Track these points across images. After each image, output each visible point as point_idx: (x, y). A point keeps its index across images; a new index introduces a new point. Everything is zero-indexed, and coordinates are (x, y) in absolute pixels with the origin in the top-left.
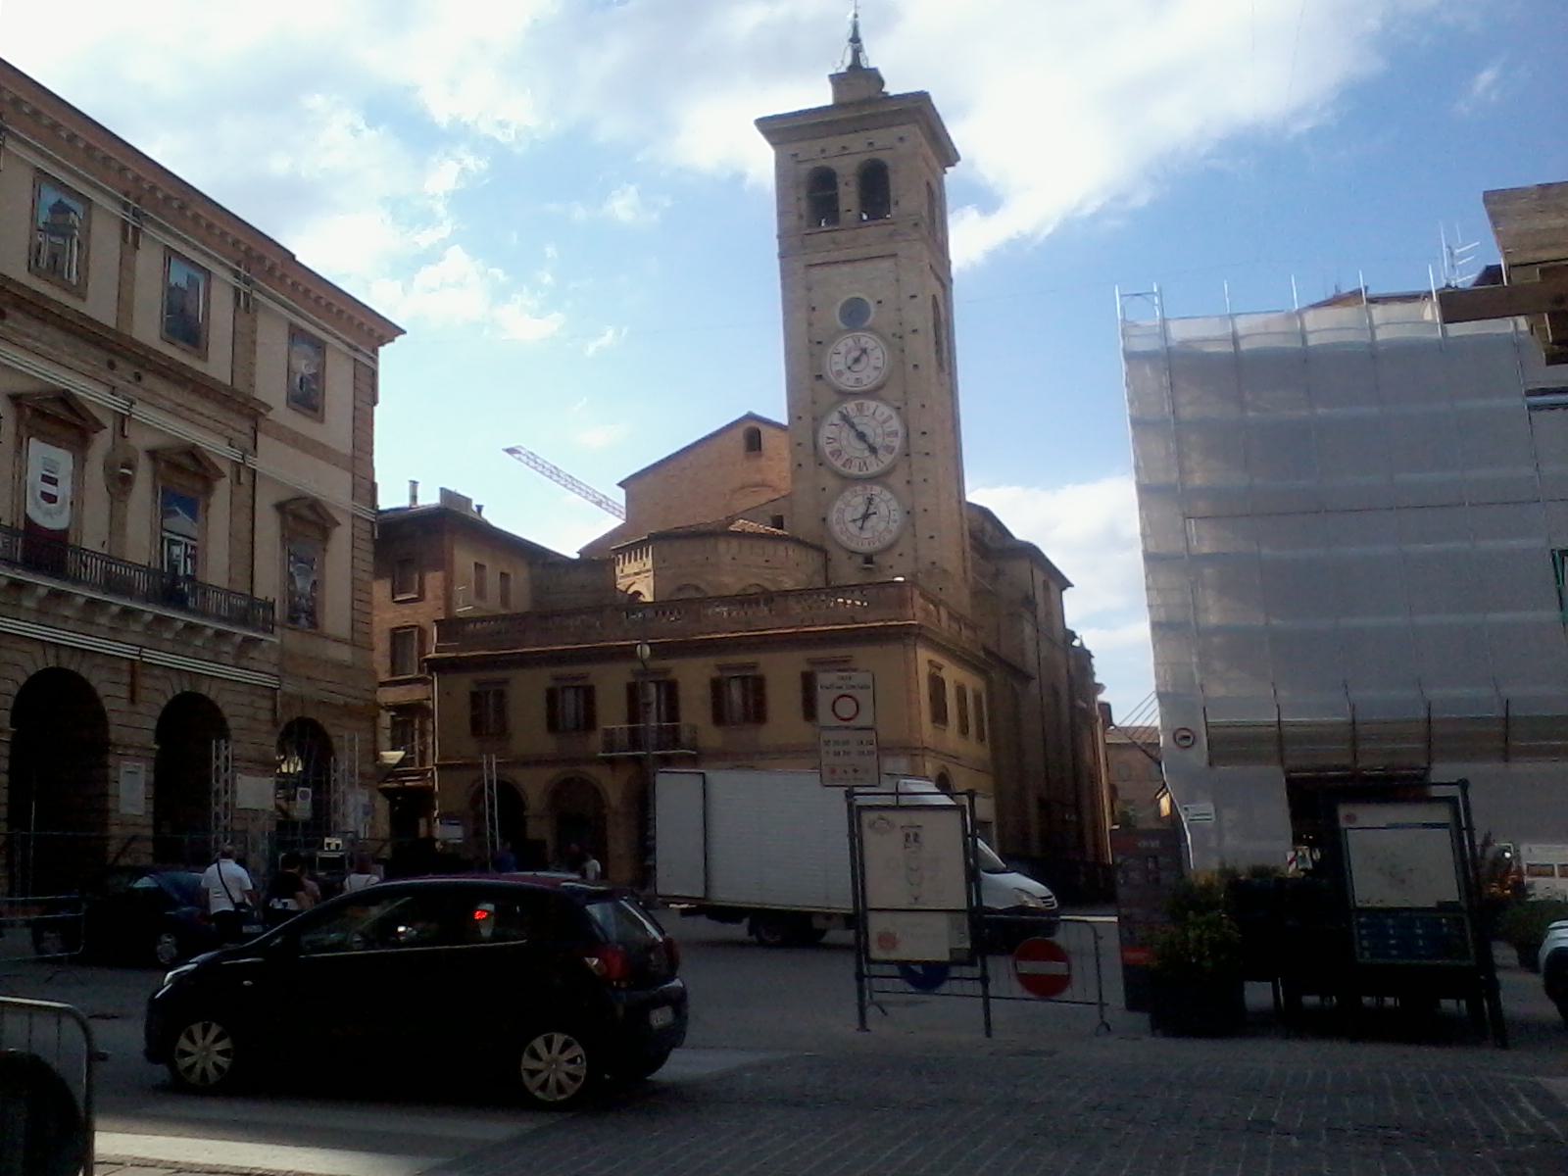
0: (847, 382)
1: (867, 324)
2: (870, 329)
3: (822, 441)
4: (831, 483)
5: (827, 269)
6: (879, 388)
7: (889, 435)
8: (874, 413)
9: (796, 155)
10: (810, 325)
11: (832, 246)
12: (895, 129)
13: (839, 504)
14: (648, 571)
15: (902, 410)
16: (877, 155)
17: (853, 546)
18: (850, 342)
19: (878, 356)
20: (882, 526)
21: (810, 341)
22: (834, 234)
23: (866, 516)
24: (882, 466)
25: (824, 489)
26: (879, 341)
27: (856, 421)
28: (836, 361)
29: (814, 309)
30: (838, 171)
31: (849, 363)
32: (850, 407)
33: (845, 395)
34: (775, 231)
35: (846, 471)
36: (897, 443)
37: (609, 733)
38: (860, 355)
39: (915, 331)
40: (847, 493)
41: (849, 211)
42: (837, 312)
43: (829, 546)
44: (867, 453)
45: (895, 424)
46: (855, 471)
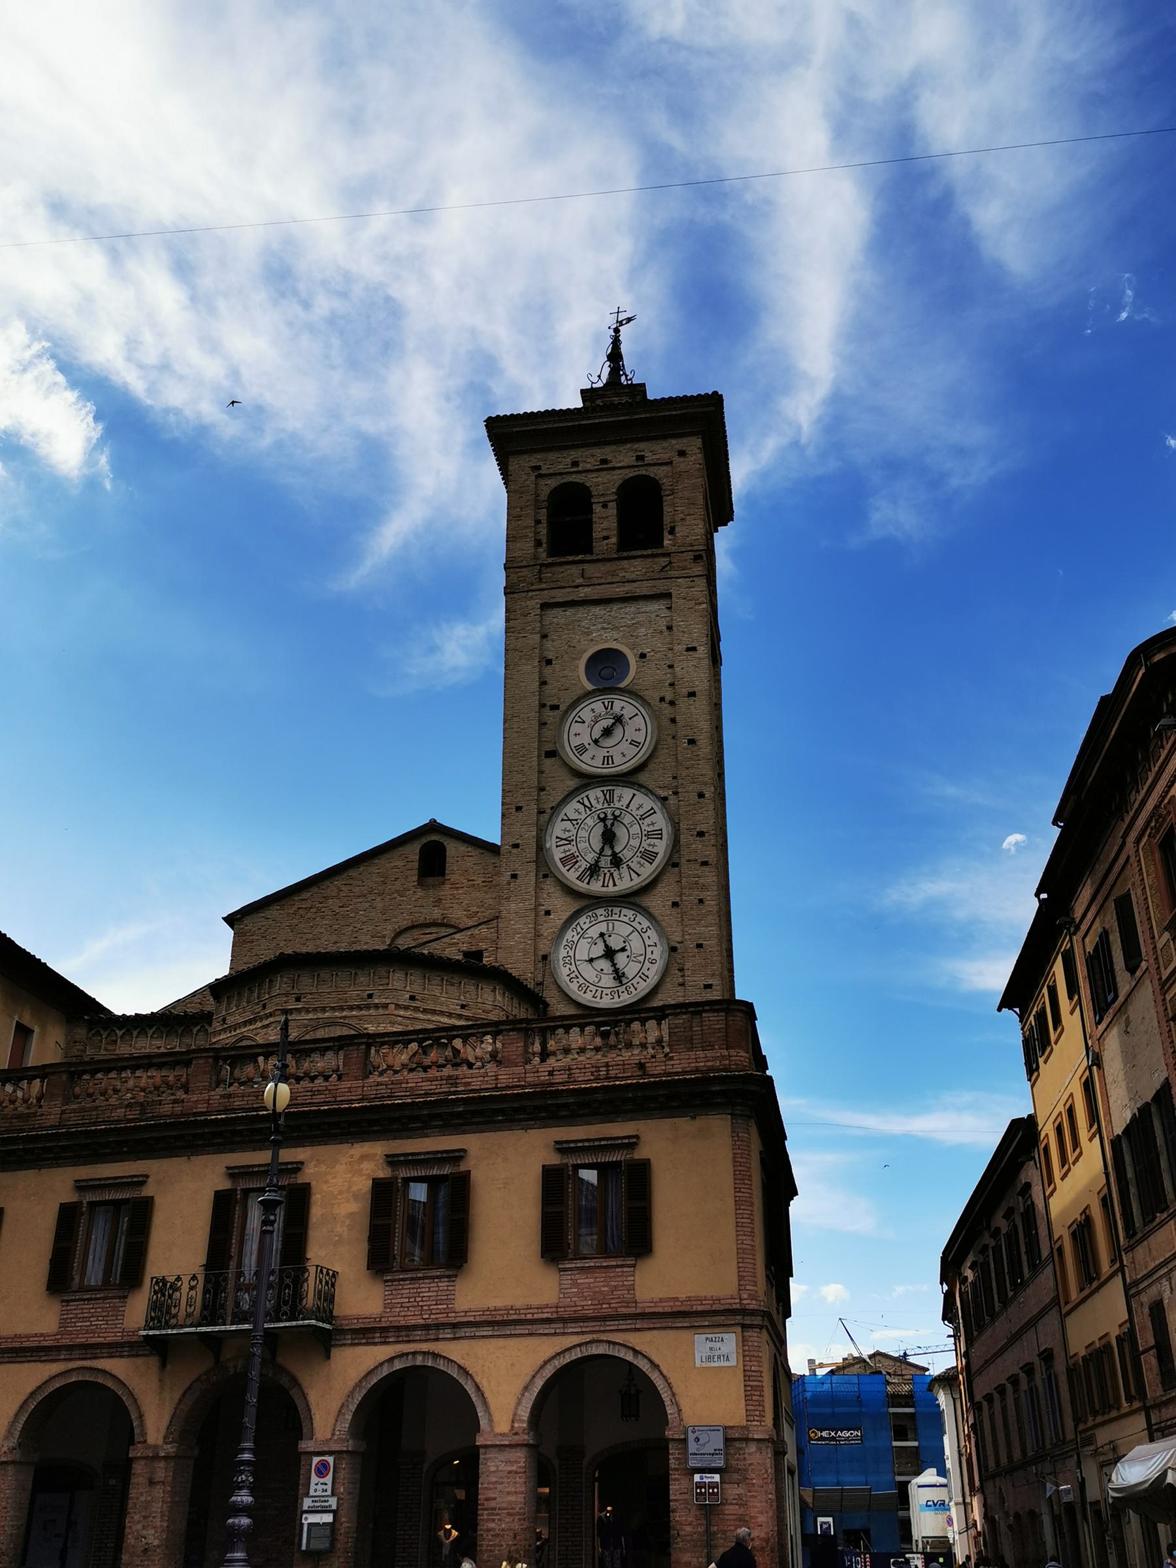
0: (591, 762)
3: (551, 843)
5: (570, 612)
6: (641, 767)
7: (648, 835)
10: (543, 683)
12: (674, 442)
13: (570, 935)
15: (672, 801)
16: (652, 472)
19: (639, 727)
22: (586, 566)
25: (548, 913)
28: (579, 732)
29: (549, 662)
31: (597, 733)
32: (595, 795)
33: (589, 780)
36: (661, 847)
37: (164, 1287)
38: (613, 724)
39: (692, 694)
40: (583, 920)
41: (606, 538)
43: (550, 996)
45: (660, 821)
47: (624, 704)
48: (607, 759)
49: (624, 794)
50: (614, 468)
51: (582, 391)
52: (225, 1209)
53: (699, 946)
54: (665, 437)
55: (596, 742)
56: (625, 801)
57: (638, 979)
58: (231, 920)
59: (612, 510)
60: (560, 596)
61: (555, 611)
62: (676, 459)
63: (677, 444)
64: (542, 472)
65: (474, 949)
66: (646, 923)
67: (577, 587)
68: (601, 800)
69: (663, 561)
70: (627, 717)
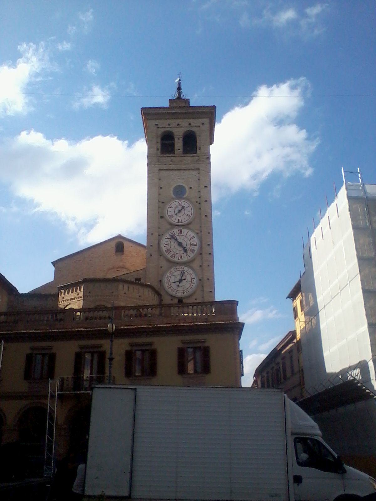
1: (184, 197)
2: (187, 199)
3: (162, 245)
4: (164, 263)
5: (168, 172)
8: (186, 235)
9: (157, 125)
10: (159, 194)
11: (171, 163)
12: (200, 120)
13: (168, 274)
14: (81, 297)
17: (174, 294)
18: (177, 203)
19: (189, 210)
20: (187, 286)
21: (159, 202)
23: (180, 281)
24: (189, 258)
25: (161, 267)
26: (189, 203)
27: (178, 237)
28: (171, 210)
29: (161, 188)
30: (175, 134)
31: (176, 212)
32: (176, 231)
33: (173, 226)
34: (146, 154)
35: (172, 259)
36: (196, 248)
38: (182, 209)
39: (206, 201)
40: (173, 270)
41: (179, 149)
42: (172, 189)
43: (162, 293)
44: (182, 252)
45: (196, 240)
46: (176, 259)
47: (184, 203)
48: (180, 220)
49: (185, 231)
50: (181, 127)
51: (170, 100)
52: (79, 357)
53: (208, 279)
54: (198, 118)
55: (176, 214)
56: (185, 234)
57: (189, 289)
58: (54, 263)
59: (181, 140)
60: (165, 167)
61: (162, 172)
62: (201, 125)
63: (201, 120)
64: (159, 126)
65: (138, 277)
66: (192, 272)
67: (170, 165)
68: (178, 232)
69: (197, 158)
70: (185, 207)
